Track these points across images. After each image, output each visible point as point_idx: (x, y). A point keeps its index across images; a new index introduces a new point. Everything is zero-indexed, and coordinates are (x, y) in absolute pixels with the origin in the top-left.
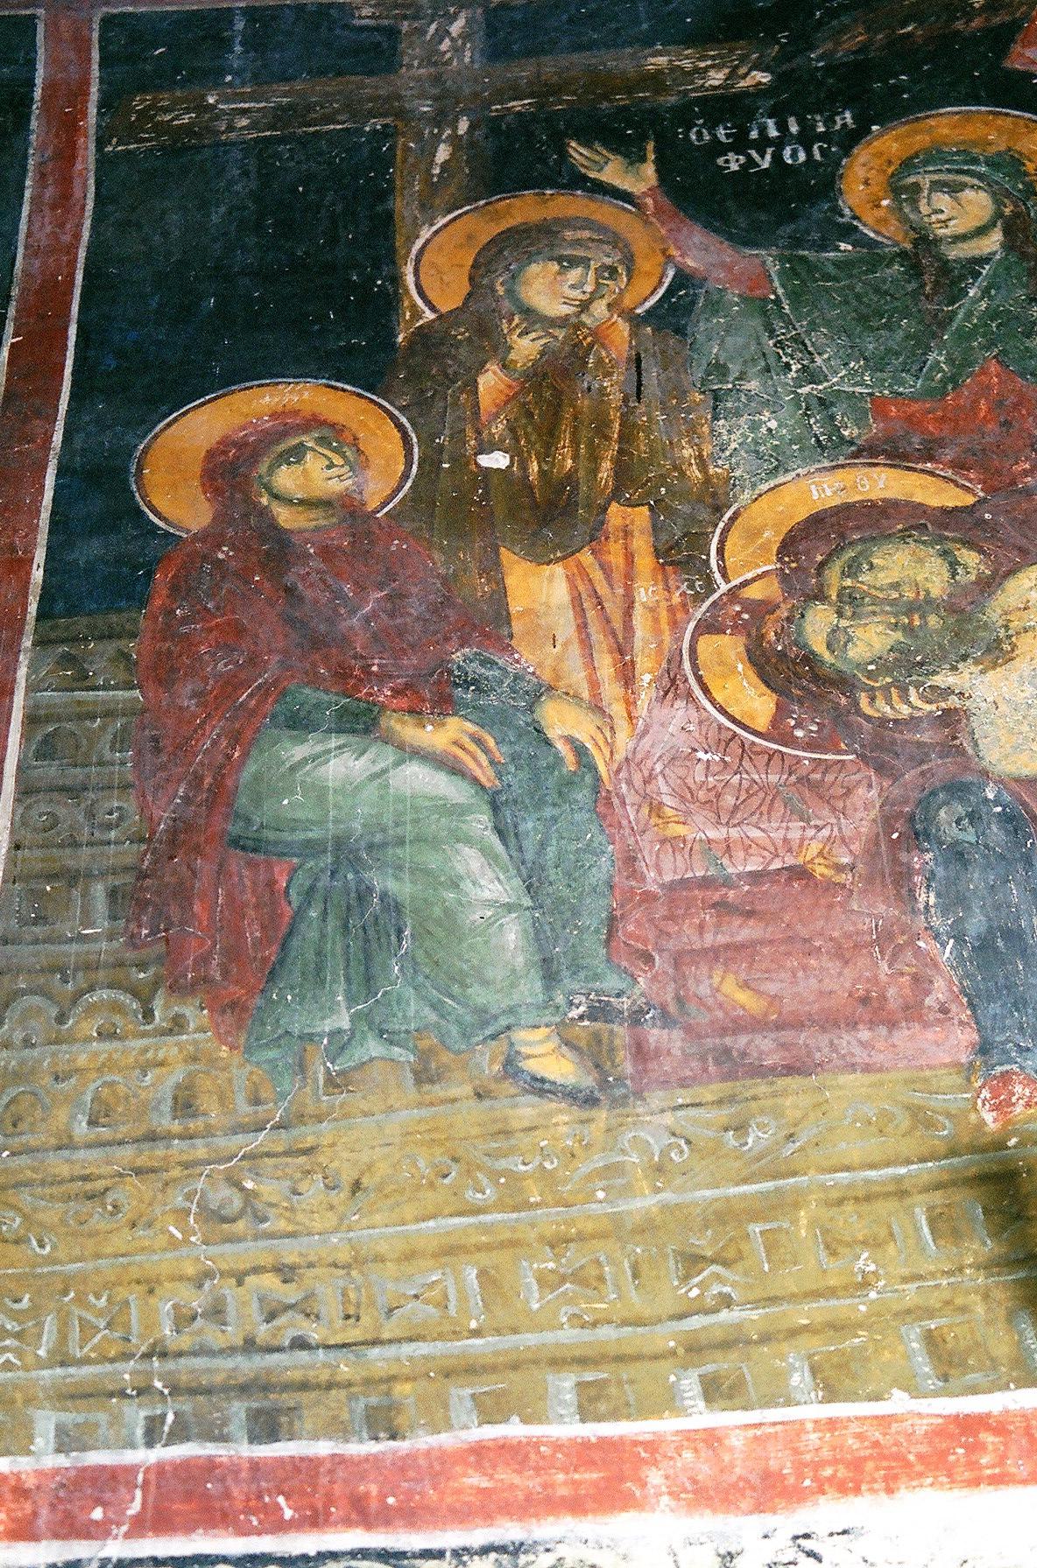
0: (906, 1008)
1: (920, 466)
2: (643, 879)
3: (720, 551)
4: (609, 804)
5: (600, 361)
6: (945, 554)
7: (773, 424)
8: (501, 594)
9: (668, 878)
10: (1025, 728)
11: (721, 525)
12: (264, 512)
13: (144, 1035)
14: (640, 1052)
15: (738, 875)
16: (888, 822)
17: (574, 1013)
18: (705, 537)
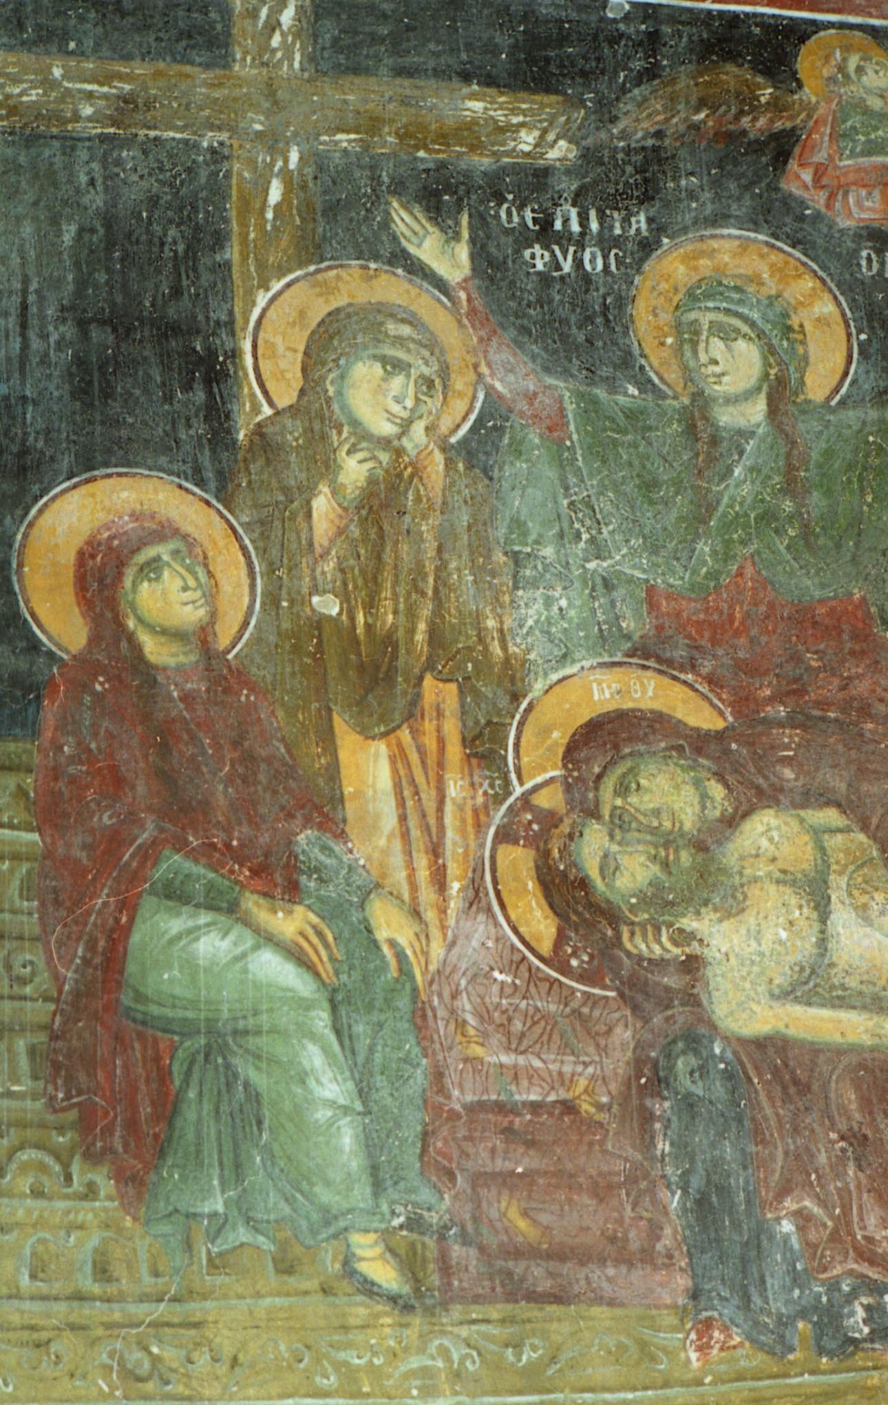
0: (643, 1251)
1: (682, 676)
2: (449, 1097)
3: (517, 745)
4: (424, 1016)
5: (418, 499)
6: (697, 783)
7: (563, 603)
8: (333, 773)
9: (469, 1098)
10: (748, 985)
11: (518, 717)
12: (131, 638)
13: (67, 1197)
14: (446, 1269)
15: (524, 1103)
16: (638, 1064)
17: (396, 1222)
18: (505, 726)
